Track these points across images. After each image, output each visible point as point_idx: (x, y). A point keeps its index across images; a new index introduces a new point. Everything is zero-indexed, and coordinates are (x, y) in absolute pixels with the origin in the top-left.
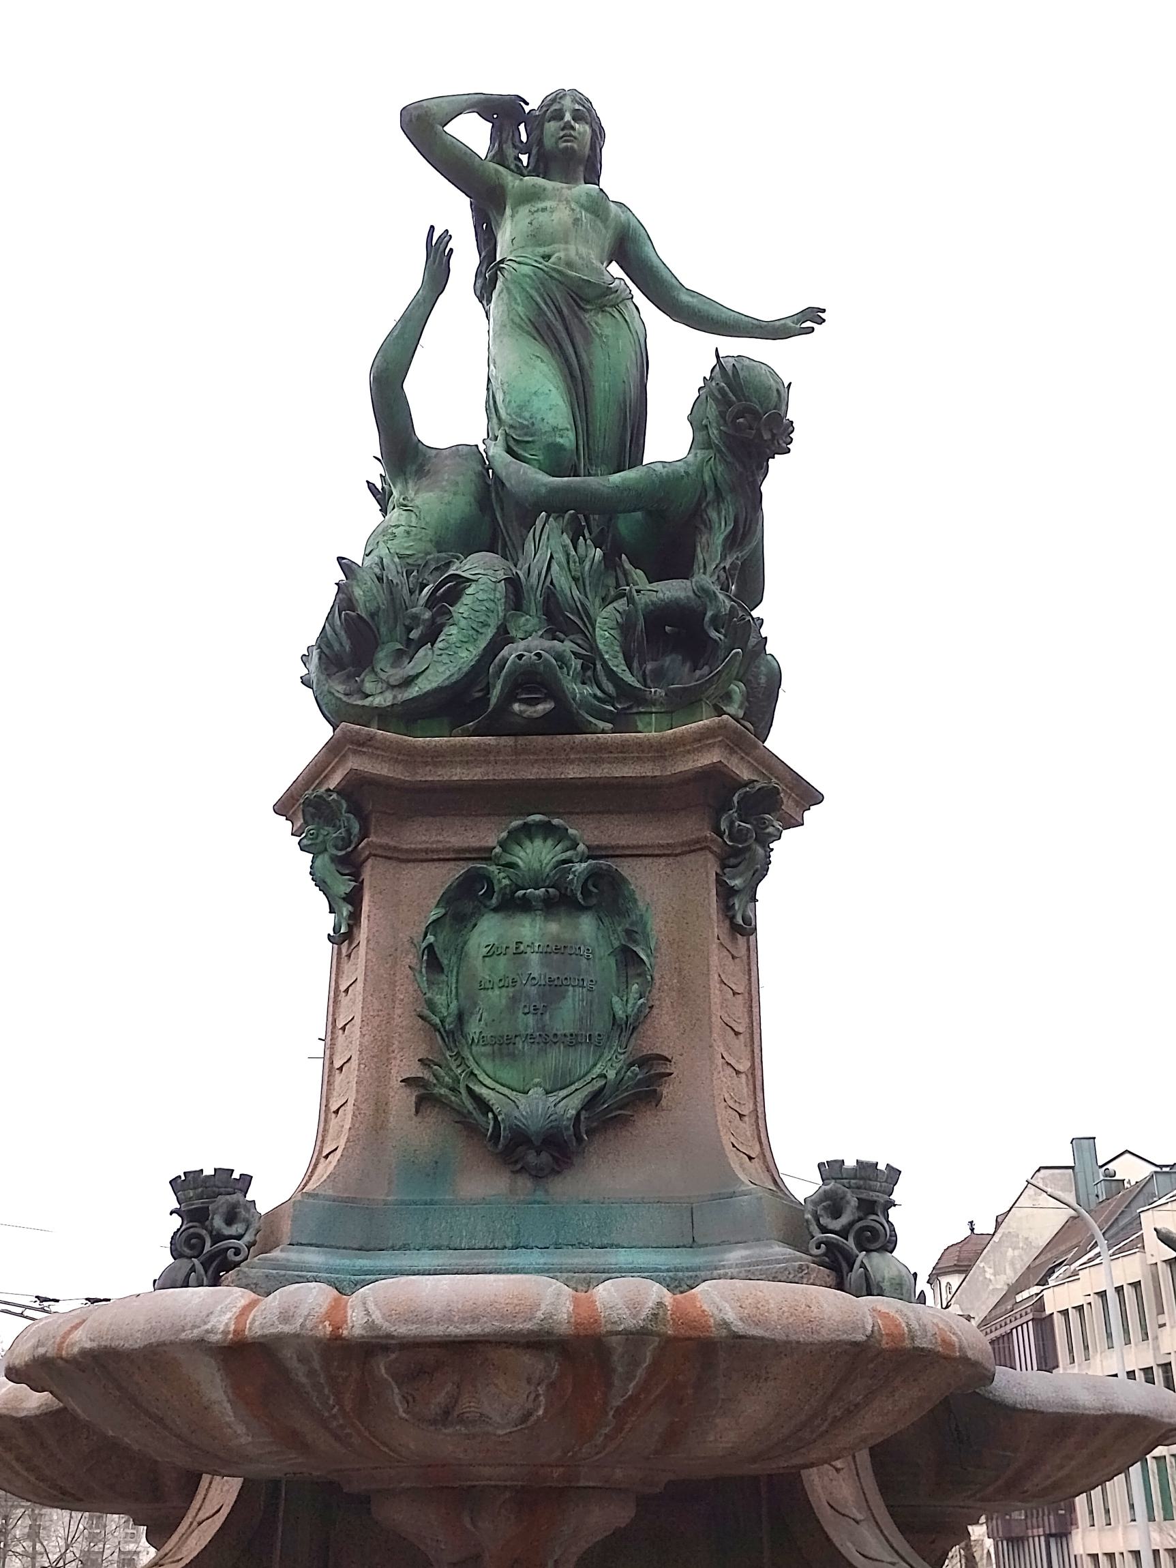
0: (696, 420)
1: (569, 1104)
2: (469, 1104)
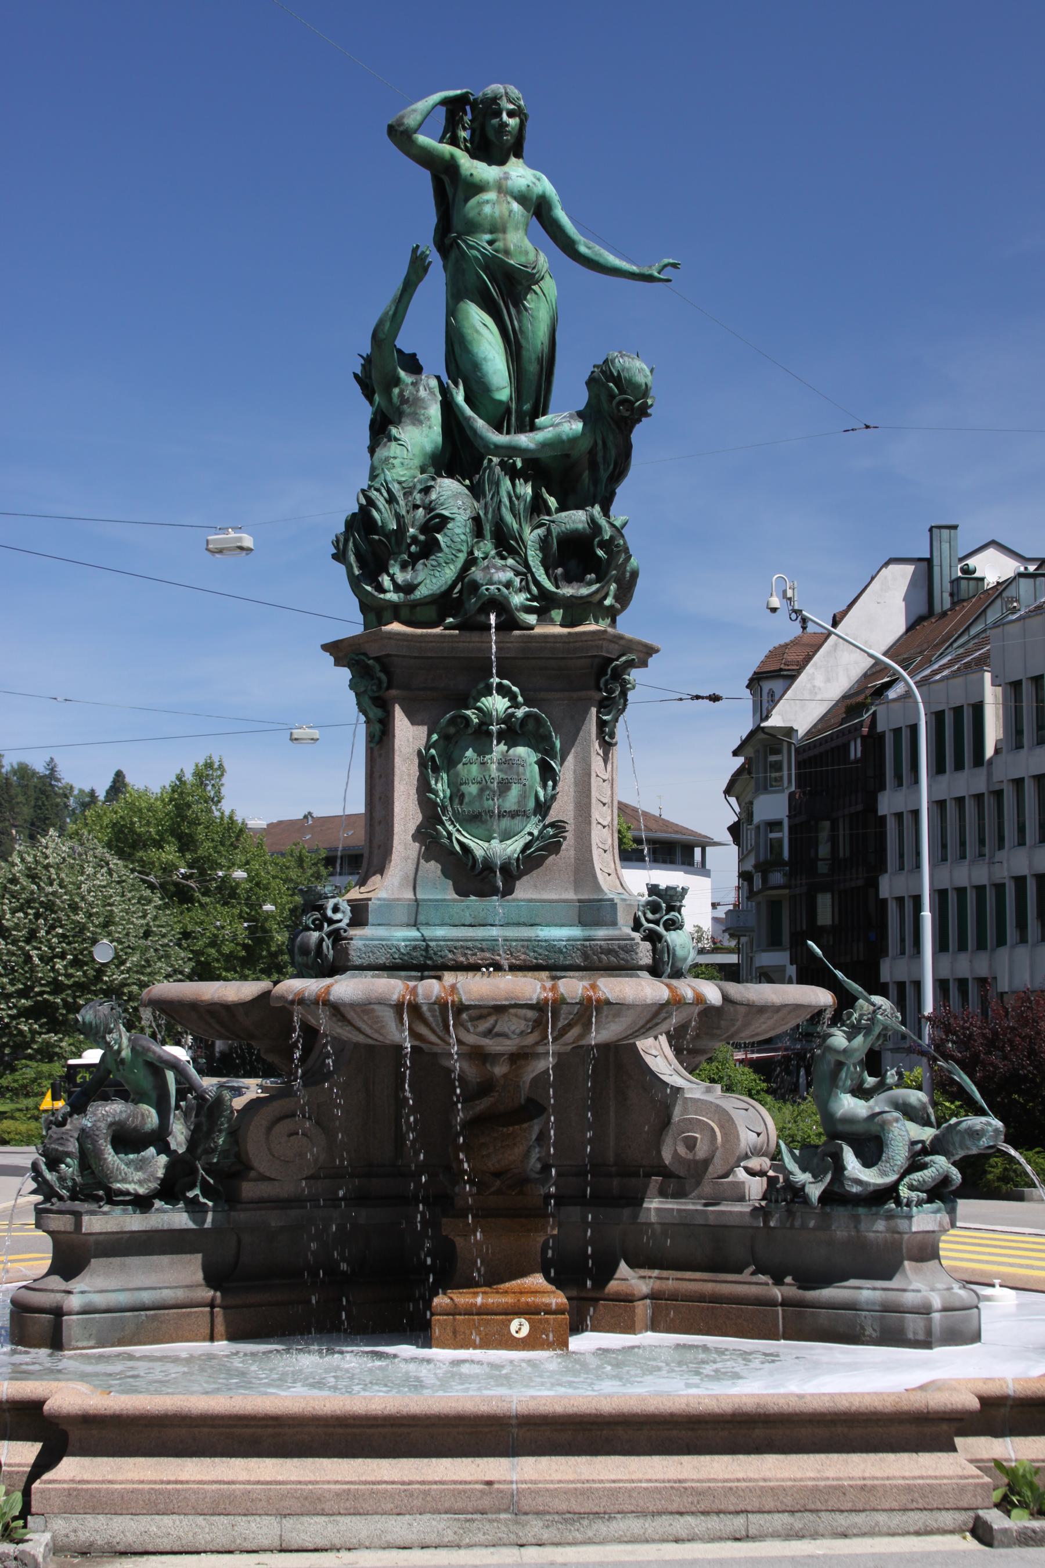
0: (592, 382)
1: (513, 847)
2: (458, 848)
